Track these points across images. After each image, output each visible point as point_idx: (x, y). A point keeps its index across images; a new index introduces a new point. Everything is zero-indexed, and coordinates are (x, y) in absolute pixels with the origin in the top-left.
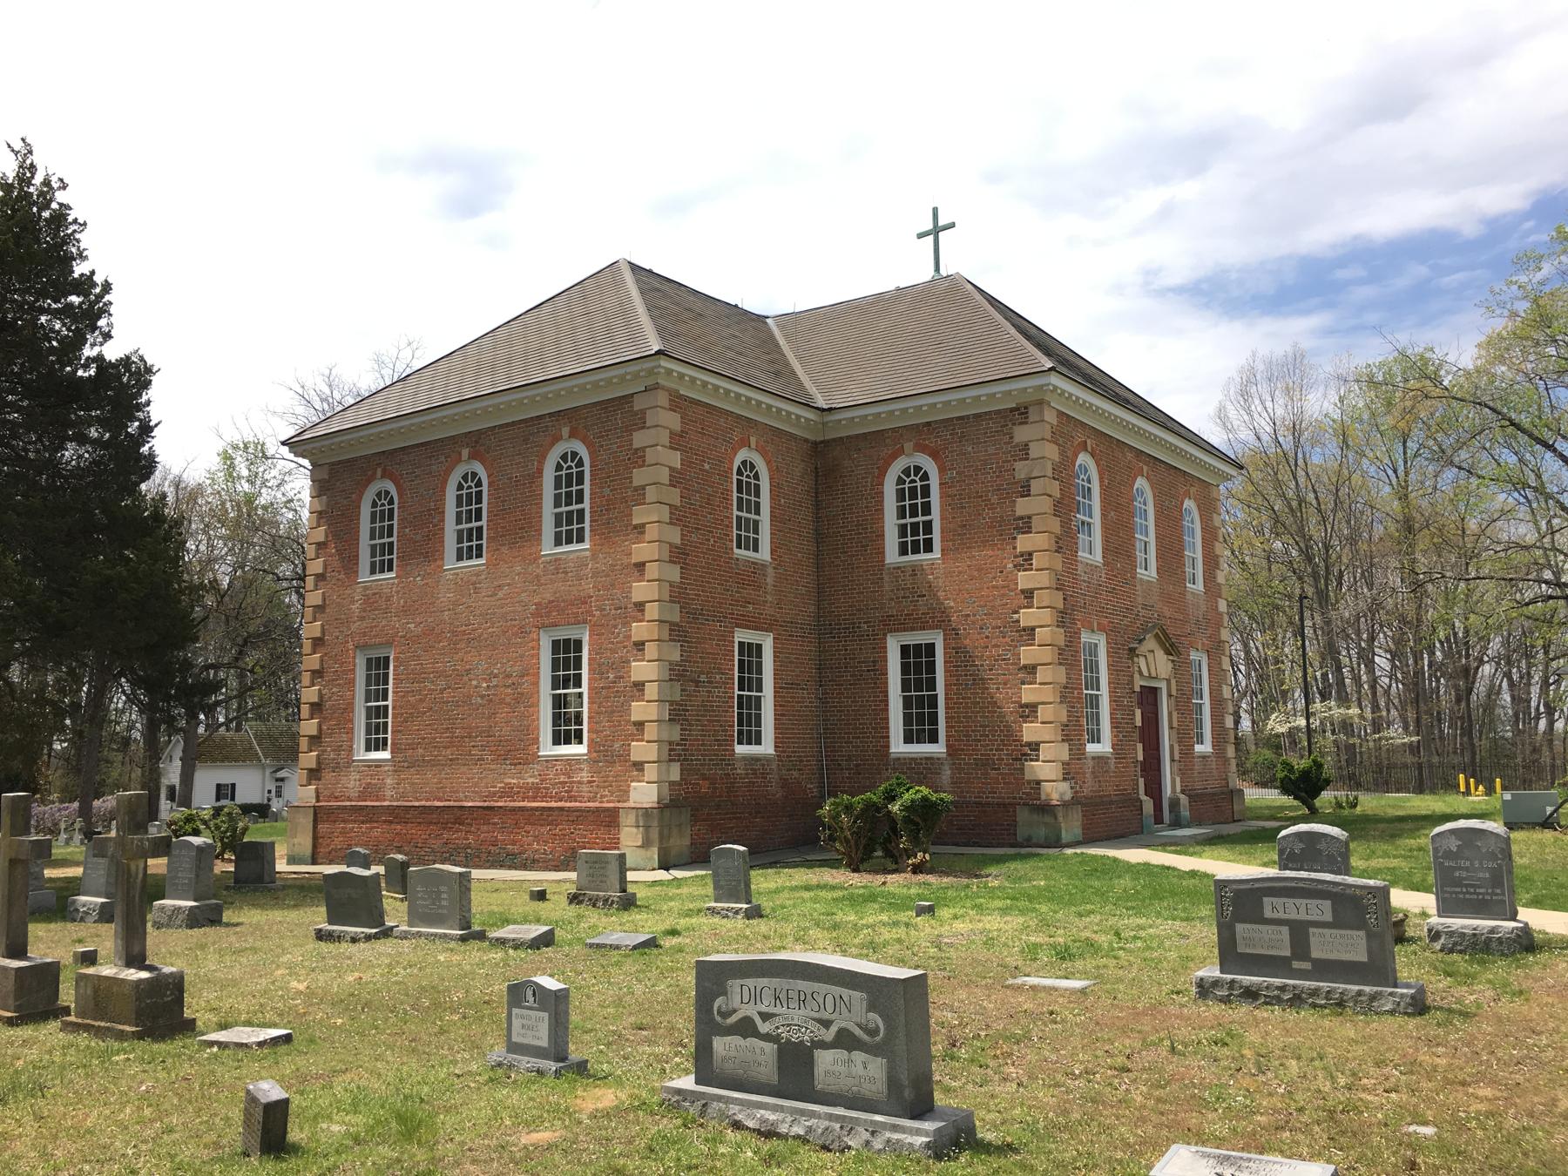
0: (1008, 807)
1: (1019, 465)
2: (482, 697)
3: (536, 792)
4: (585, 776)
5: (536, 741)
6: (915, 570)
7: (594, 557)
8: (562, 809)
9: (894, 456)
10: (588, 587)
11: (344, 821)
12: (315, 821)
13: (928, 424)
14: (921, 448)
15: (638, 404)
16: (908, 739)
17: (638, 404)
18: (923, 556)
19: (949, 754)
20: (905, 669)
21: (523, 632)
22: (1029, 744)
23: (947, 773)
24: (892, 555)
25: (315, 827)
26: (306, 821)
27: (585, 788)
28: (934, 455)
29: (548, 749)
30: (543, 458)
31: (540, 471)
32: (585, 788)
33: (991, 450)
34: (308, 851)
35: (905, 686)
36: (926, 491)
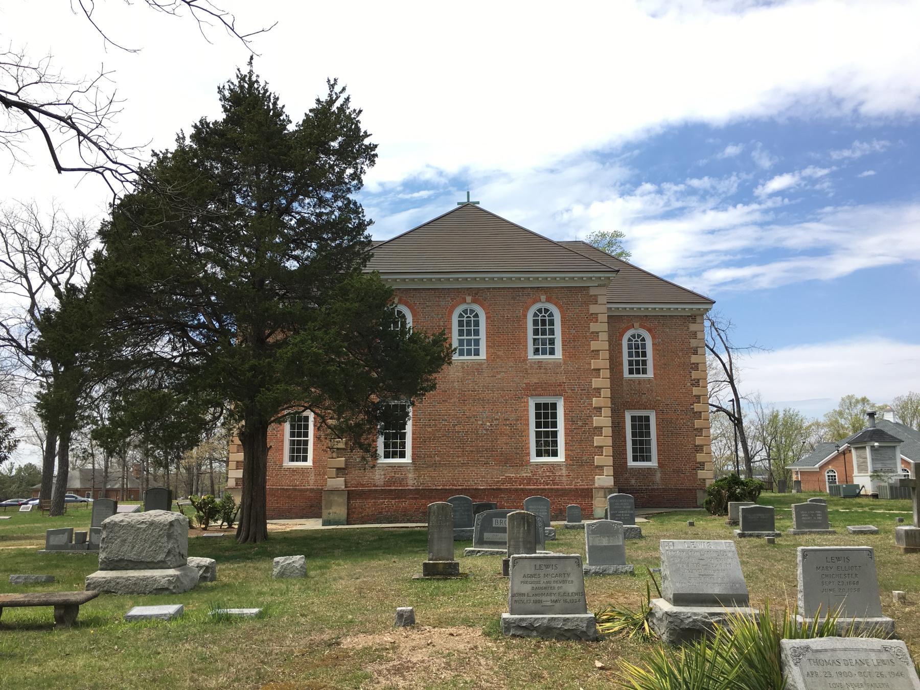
0: (692, 491)
1: (692, 341)
2: (487, 430)
3: (529, 480)
4: (564, 472)
5: (528, 454)
6: (640, 382)
7: (565, 363)
8: (552, 489)
9: (628, 328)
10: (563, 378)
11: (375, 499)
12: (349, 499)
13: (646, 316)
14: (642, 326)
15: (592, 292)
16: (635, 459)
17: (592, 292)
18: (641, 376)
19: (659, 466)
20: (633, 427)
21: (518, 398)
22: (699, 463)
23: (658, 475)
24: (626, 374)
25: (348, 503)
26: (343, 499)
27: (564, 479)
28: (650, 330)
29: (534, 459)
30: (527, 309)
31: (525, 316)
32: (564, 479)
33: (678, 332)
34: (345, 516)
35: (634, 434)
36: (644, 346)
